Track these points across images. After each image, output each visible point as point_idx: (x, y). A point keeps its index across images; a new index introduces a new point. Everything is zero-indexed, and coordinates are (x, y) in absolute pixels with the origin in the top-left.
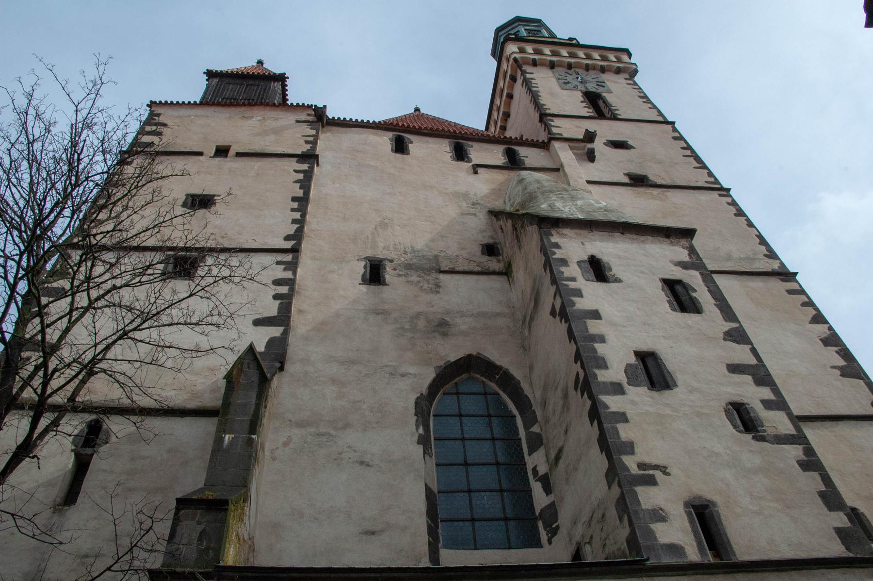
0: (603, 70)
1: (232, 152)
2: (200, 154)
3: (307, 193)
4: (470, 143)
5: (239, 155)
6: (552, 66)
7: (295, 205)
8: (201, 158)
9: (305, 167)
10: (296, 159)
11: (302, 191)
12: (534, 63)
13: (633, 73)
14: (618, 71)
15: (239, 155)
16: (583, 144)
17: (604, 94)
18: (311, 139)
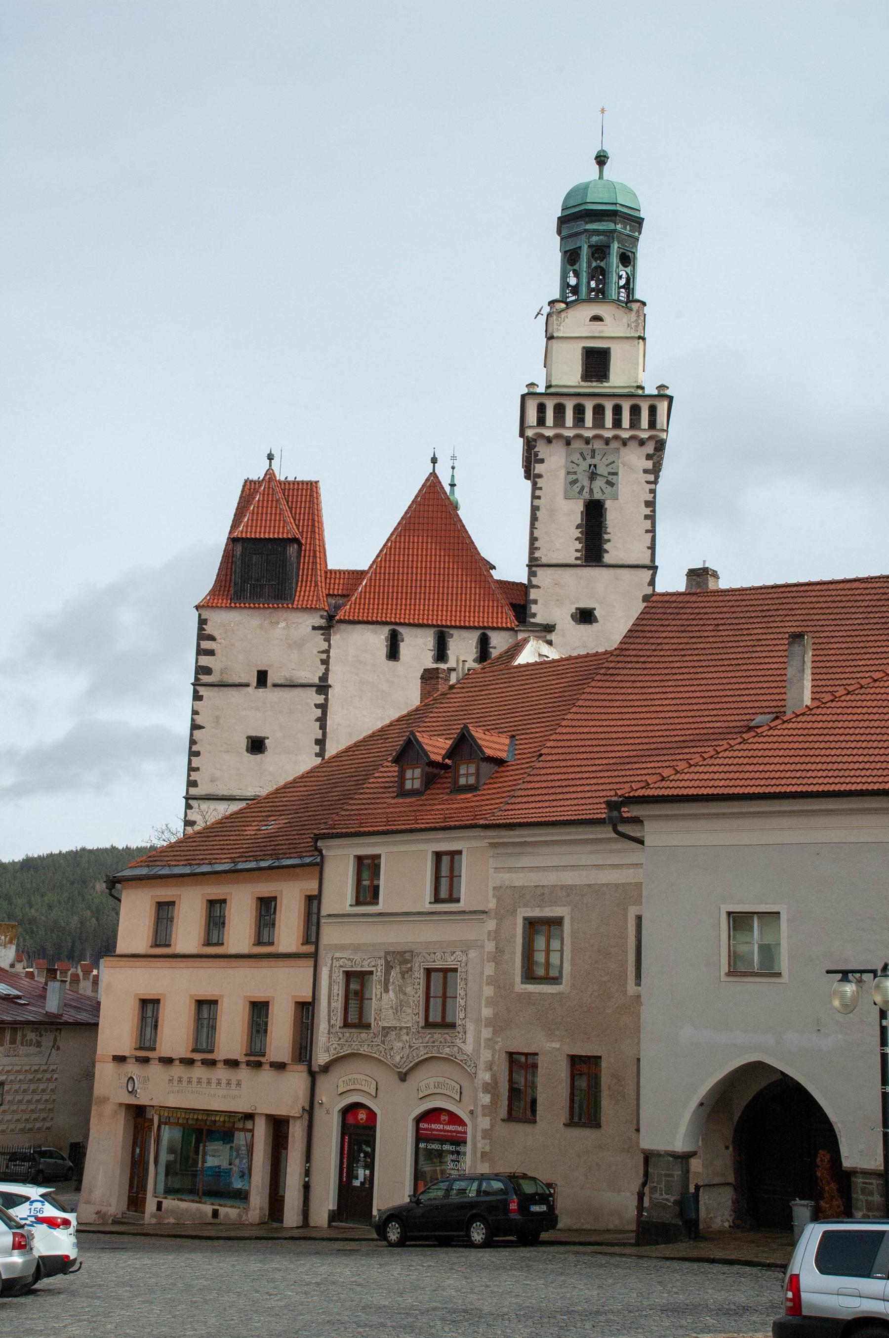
0: (625, 443)
1: (270, 682)
2: (247, 685)
3: (324, 734)
4: (452, 631)
5: (275, 685)
6: (568, 442)
7: (317, 749)
8: (250, 689)
9: (320, 699)
10: (315, 689)
11: (321, 731)
14: (642, 443)
15: (275, 685)
16: (544, 634)
17: (608, 504)
18: (324, 656)
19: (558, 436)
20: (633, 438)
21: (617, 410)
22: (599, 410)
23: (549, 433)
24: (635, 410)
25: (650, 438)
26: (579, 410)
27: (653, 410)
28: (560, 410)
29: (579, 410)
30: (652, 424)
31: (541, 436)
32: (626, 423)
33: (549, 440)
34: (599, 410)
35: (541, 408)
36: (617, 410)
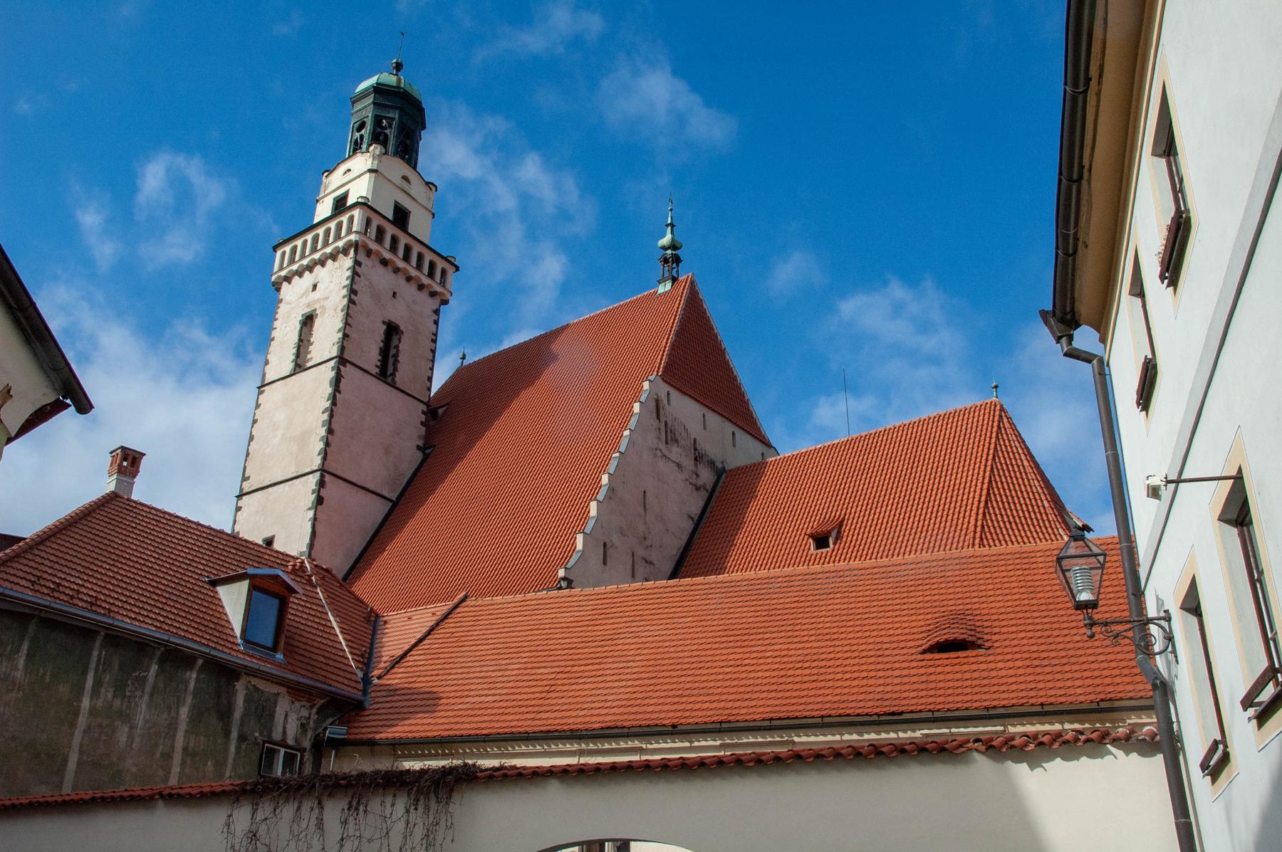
13: (445, 302)
14: (433, 294)
30: (443, 283)
33: (369, 253)
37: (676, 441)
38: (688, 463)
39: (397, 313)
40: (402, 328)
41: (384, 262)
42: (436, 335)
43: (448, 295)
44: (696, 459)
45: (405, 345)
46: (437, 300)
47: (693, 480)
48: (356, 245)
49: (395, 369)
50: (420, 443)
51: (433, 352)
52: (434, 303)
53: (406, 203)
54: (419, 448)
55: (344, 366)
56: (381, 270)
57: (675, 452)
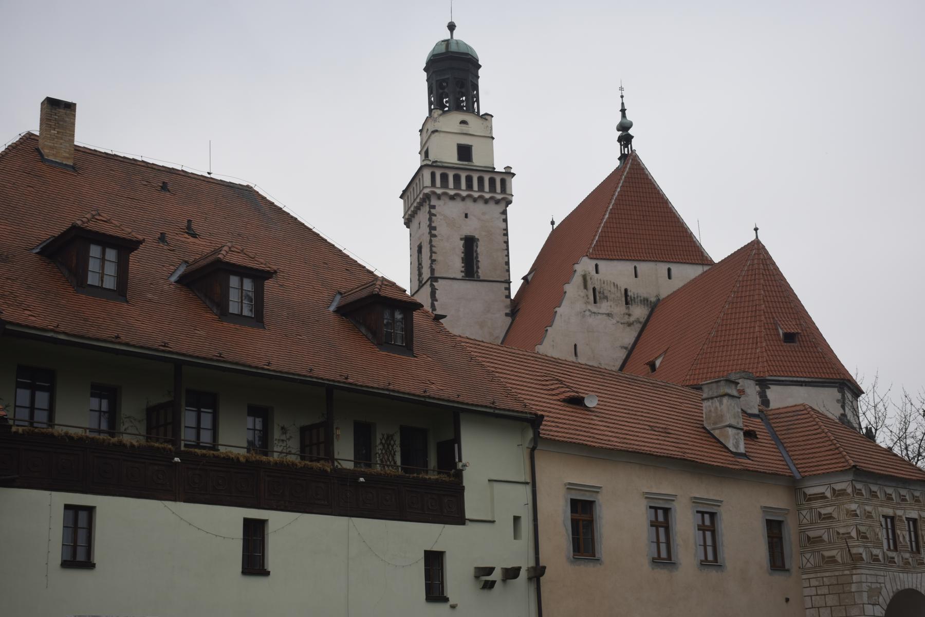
12: (439, 197)
14: (497, 202)
19: (445, 194)
20: (492, 198)
21: (481, 180)
22: (469, 179)
23: (439, 191)
24: (492, 181)
25: (503, 199)
26: (457, 178)
27: (503, 182)
28: (444, 177)
29: (457, 178)
31: (434, 193)
32: (487, 188)
34: (469, 179)
35: (433, 175)
36: (481, 180)
37: (606, 298)
38: (621, 309)
39: (470, 227)
40: (477, 237)
41: (452, 198)
42: (506, 230)
43: (509, 197)
44: (627, 303)
45: (482, 249)
46: (503, 204)
47: (626, 319)
48: (427, 197)
49: (478, 268)
50: (508, 311)
51: (507, 243)
52: (500, 208)
53: (465, 141)
54: (507, 315)
55: (436, 281)
56: (451, 204)
57: (604, 307)
